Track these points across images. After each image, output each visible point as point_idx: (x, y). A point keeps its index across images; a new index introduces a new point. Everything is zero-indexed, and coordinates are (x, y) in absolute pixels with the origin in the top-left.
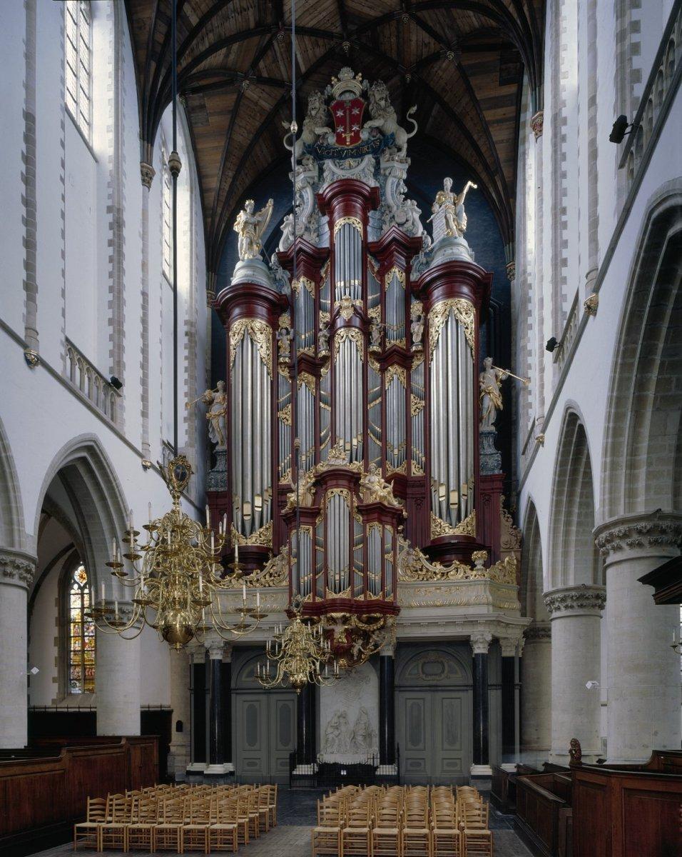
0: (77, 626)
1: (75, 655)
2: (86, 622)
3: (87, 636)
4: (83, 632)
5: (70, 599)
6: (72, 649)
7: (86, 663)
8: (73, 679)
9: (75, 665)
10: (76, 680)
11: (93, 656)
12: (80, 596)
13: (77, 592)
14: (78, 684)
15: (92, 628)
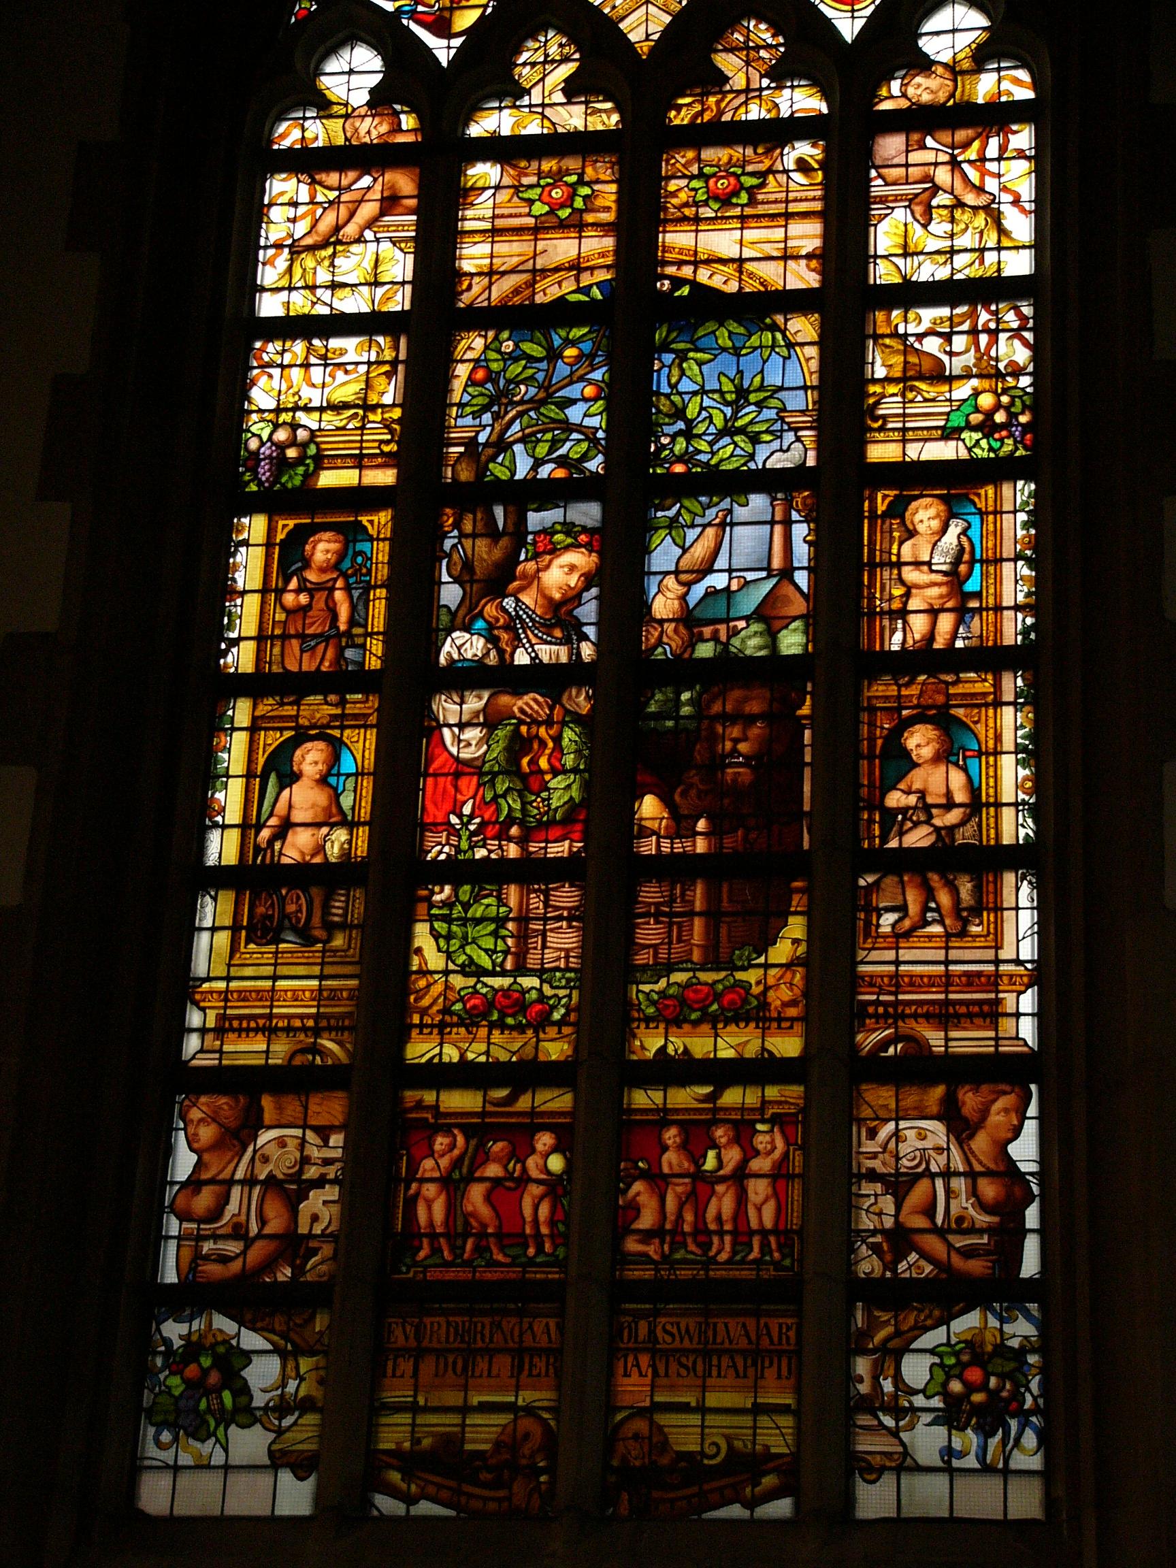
0: (323, 549)
1: (254, 929)
2: (481, 493)
3: (464, 678)
4: (417, 623)
5: (257, 213)
6: (222, 848)
7: (420, 1050)
8: (193, 1296)
9: (246, 1084)
10: (247, 1297)
11: (563, 941)
12: (405, 183)
13: (371, 130)
14: (263, 1374)
15: (562, 572)
